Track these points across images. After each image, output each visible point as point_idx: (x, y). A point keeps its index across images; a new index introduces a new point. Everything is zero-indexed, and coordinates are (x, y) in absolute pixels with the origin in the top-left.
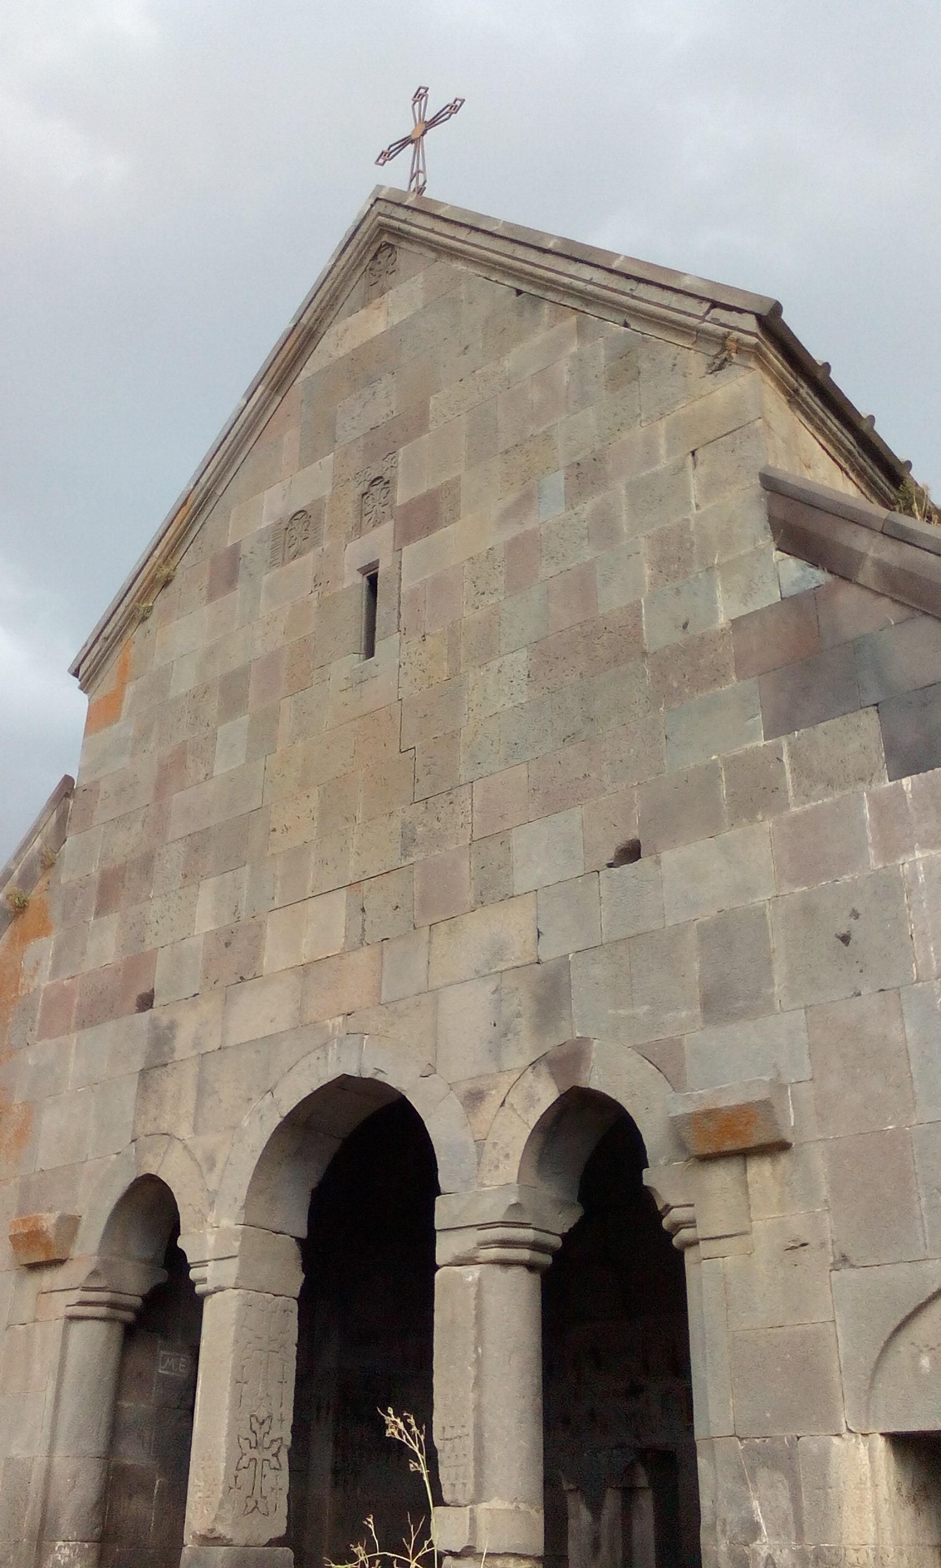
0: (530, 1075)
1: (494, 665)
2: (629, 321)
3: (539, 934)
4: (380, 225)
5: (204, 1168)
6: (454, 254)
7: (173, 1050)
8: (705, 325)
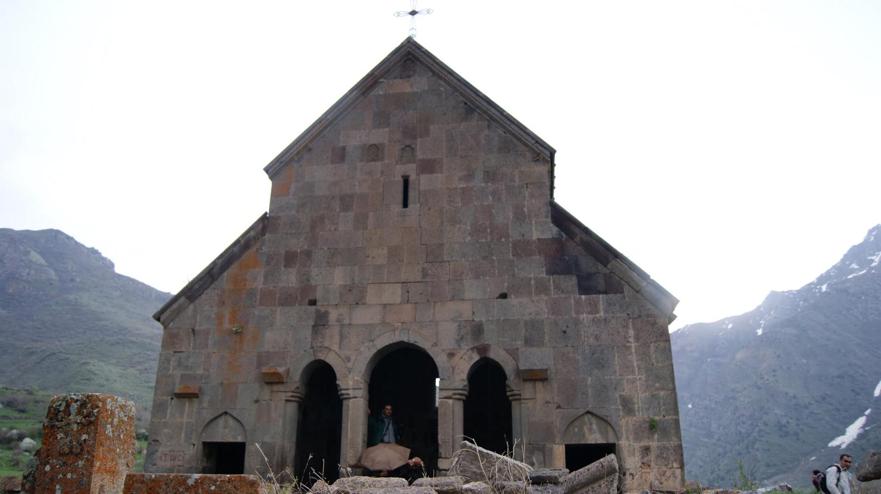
0: (470, 352)
1: (458, 226)
2: (506, 132)
3: (473, 312)
4: (409, 51)
5: (346, 361)
6: (440, 77)
7: (328, 321)
8: (533, 147)
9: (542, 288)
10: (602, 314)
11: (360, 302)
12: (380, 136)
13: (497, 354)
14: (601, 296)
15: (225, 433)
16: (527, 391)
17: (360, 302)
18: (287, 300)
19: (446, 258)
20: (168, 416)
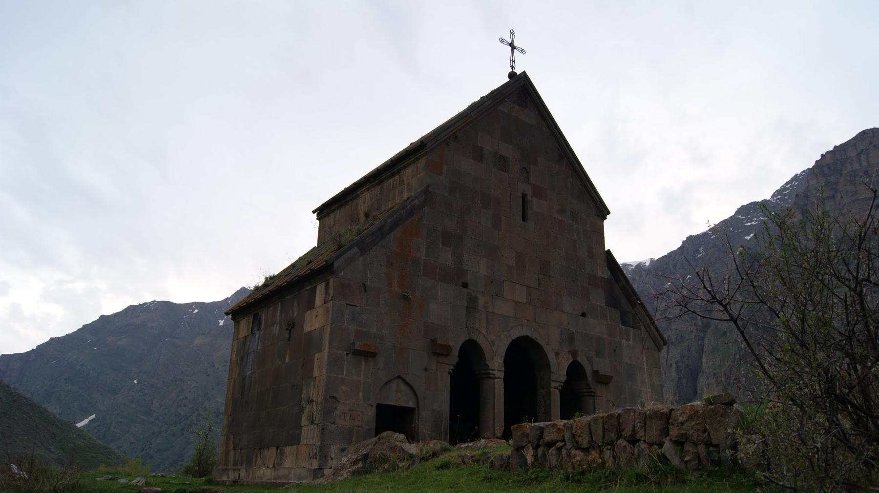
13: (582, 360)
14: (631, 329)
15: (398, 397)
16: (599, 390)
20: (345, 373)
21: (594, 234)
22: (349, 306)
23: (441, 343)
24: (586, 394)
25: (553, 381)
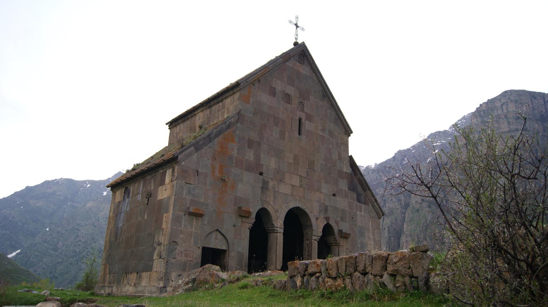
7: (268, 187)
9: (346, 196)
10: (363, 213)
11: (281, 181)
12: (290, 90)
13: (332, 223)
15: (216, 243)
16: (342, 242)
17: (281, 181)
18: (249, 168)
19: (316, 169)
21: (342, 145)
22: (187, 184)
23: (245, 210)
24: (334, 244)
25: (314, 235)
